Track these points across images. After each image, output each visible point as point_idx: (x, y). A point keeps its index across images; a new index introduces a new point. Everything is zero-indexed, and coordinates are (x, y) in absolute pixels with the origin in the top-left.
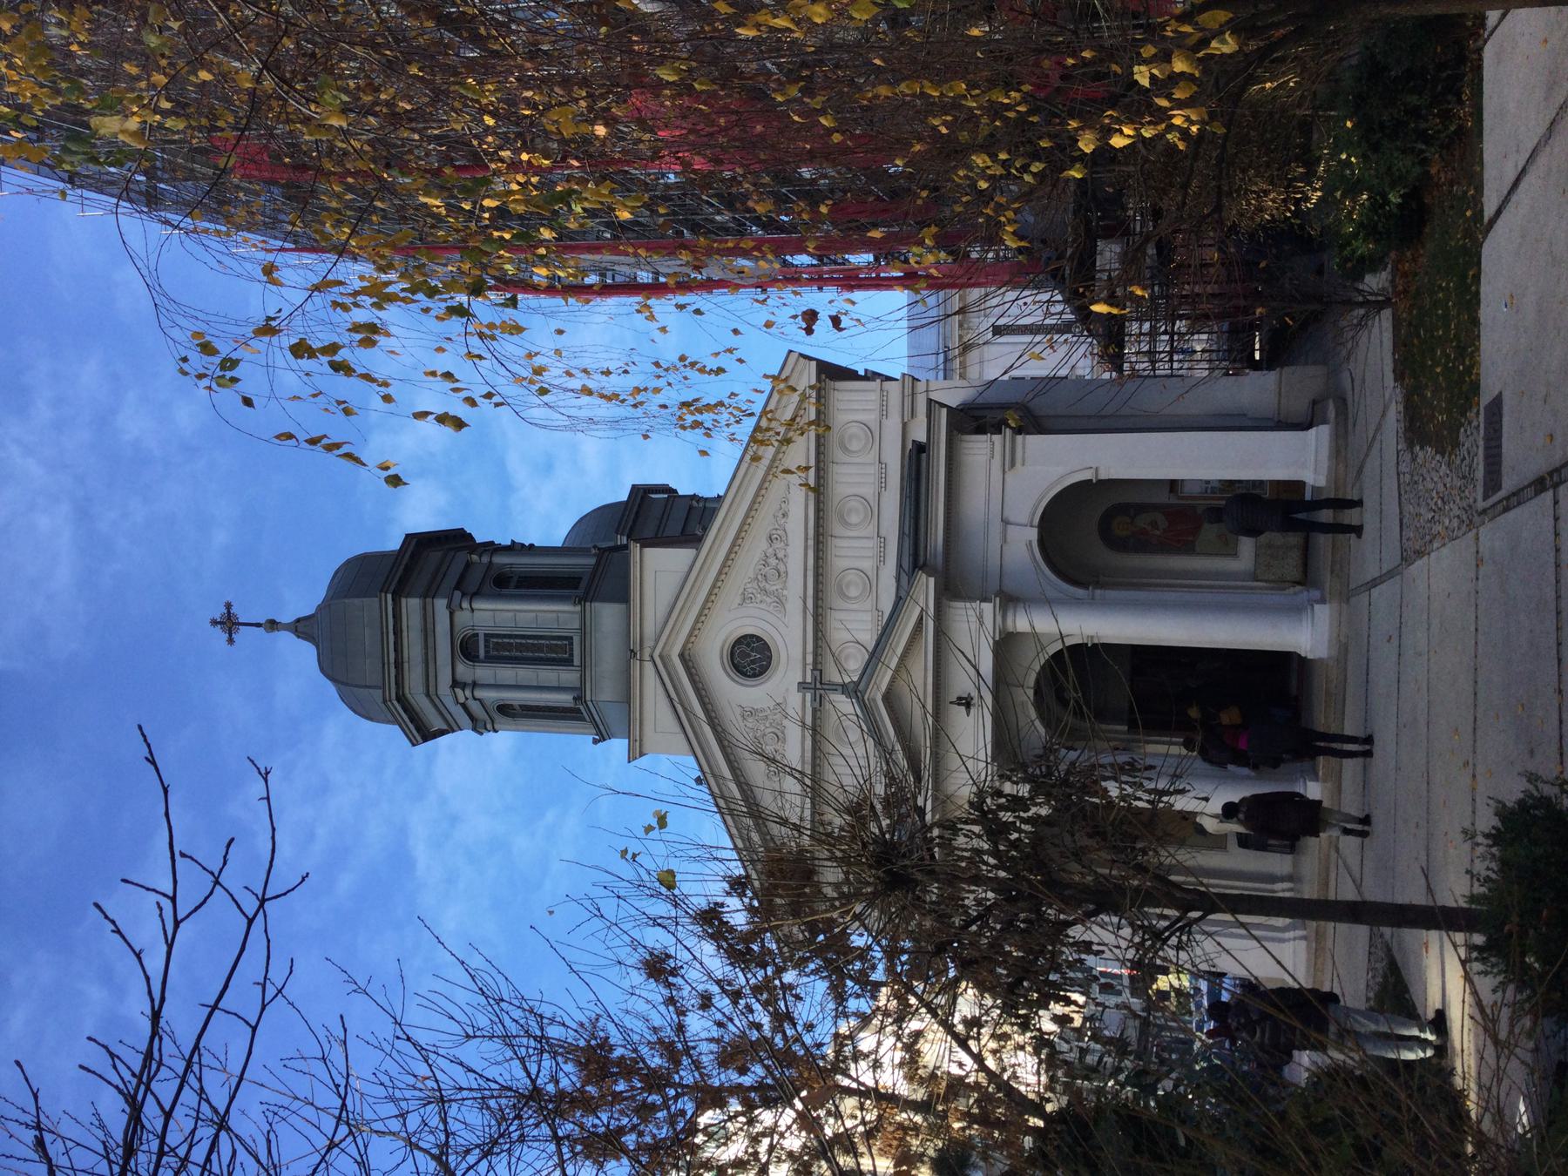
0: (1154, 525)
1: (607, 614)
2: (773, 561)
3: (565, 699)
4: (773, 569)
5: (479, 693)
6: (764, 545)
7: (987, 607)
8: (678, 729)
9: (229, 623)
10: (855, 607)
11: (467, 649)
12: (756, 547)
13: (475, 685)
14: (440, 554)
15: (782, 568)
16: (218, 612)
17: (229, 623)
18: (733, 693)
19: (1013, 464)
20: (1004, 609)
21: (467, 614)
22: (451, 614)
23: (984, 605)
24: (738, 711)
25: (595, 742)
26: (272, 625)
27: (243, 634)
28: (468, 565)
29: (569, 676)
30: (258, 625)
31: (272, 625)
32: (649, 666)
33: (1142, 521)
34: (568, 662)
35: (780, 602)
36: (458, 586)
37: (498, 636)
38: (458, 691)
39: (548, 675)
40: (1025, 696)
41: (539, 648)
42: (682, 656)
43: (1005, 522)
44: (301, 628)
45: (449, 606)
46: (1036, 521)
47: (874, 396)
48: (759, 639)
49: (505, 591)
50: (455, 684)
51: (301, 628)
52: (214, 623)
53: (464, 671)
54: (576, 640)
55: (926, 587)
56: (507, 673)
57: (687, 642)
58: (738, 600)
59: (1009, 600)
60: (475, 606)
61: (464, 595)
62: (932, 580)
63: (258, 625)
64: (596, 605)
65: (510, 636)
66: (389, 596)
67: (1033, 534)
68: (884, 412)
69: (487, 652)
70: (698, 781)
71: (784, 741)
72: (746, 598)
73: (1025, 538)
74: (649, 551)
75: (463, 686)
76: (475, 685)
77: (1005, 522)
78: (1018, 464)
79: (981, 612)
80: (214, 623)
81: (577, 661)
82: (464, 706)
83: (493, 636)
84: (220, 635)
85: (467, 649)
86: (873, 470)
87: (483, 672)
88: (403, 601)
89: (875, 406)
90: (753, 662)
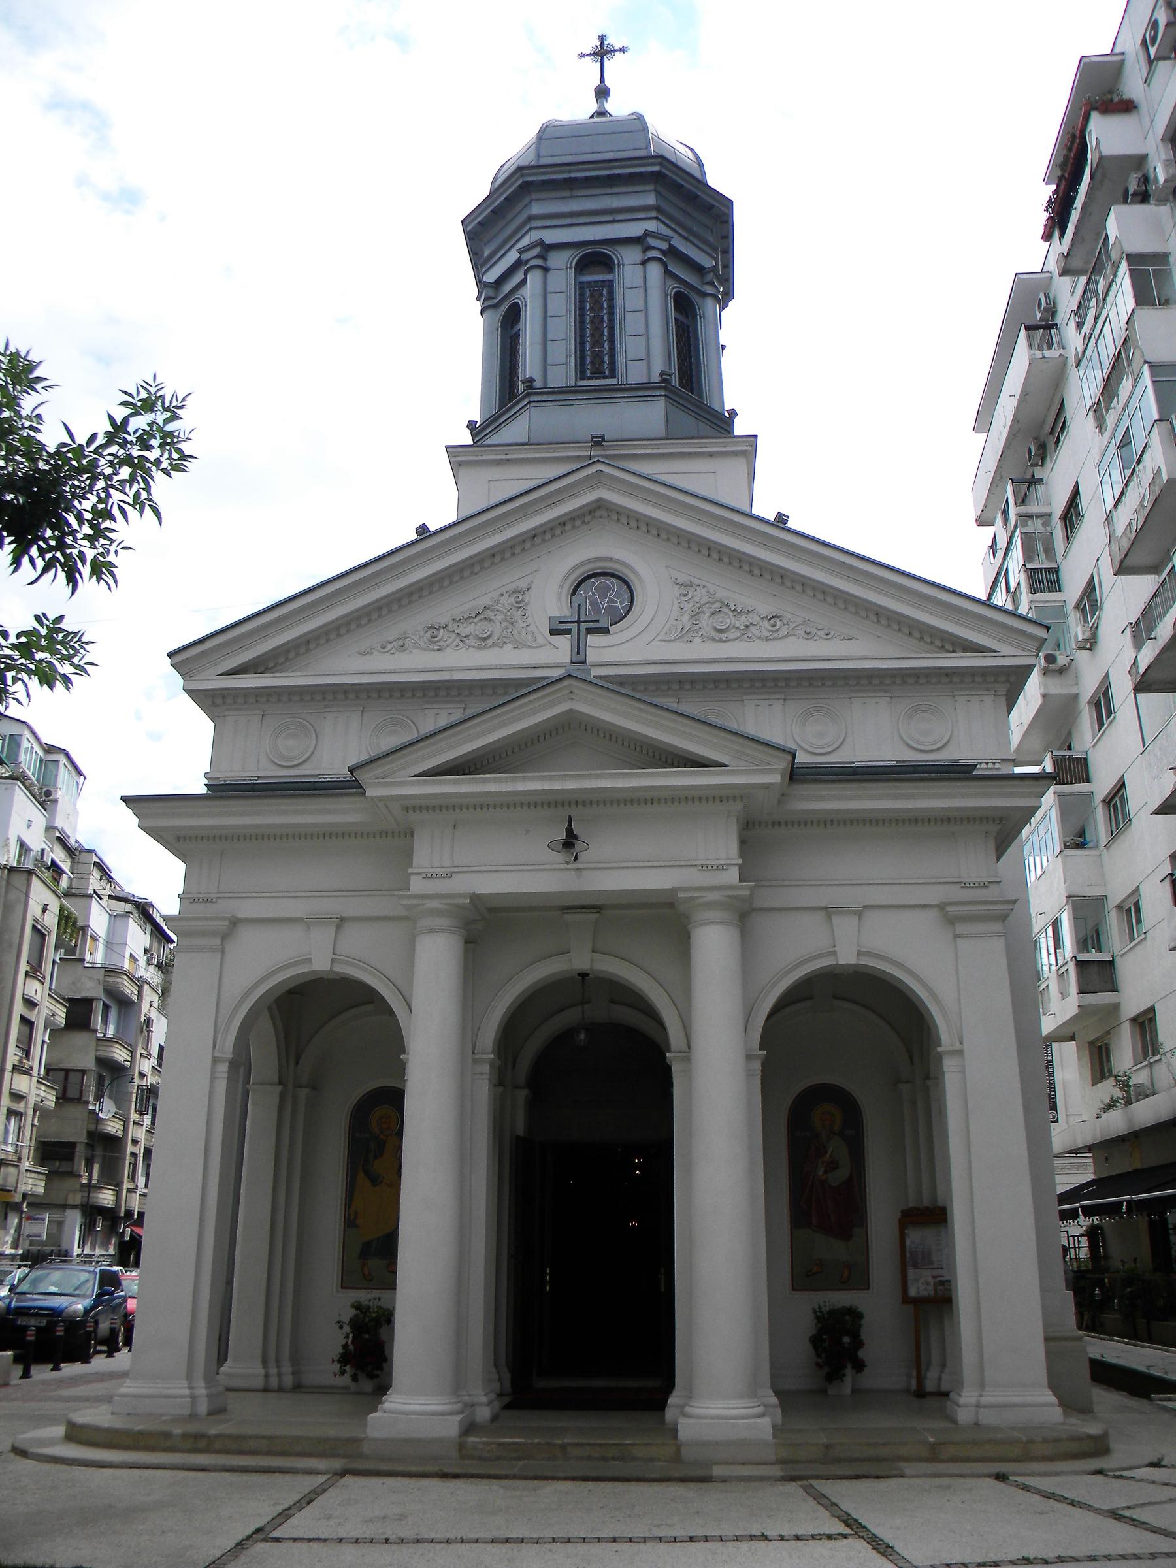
0: (833, 1166)
3: (529, 366)
7: (732, 876)
8: (493, 502)
9: (602, 52)
13: (546, 270)
15: (732, 634)
16: (614, 41)
17: (602, 52)
24: (522, 584)
25: (471, 425)
29: (561, 376)
30: (602, 80)
33: (837, 1149)
35: (685, 636)
41: (597, 342)
42: (600, 504)
45: (647, 234)
46: (865, 961)
50: (547, 248)
52: (602, 38)
54: (613, 381)
58: (683, 578)
61: (663, 252)
62: (776, 779)
63: (602, 80)
65: (611, 307)
66: (657, 168)
67: (847, 957)
71: (480, 648)
76: (546, 270)
79: (723, 867)
80: (602, 38)
88: (650, 187)
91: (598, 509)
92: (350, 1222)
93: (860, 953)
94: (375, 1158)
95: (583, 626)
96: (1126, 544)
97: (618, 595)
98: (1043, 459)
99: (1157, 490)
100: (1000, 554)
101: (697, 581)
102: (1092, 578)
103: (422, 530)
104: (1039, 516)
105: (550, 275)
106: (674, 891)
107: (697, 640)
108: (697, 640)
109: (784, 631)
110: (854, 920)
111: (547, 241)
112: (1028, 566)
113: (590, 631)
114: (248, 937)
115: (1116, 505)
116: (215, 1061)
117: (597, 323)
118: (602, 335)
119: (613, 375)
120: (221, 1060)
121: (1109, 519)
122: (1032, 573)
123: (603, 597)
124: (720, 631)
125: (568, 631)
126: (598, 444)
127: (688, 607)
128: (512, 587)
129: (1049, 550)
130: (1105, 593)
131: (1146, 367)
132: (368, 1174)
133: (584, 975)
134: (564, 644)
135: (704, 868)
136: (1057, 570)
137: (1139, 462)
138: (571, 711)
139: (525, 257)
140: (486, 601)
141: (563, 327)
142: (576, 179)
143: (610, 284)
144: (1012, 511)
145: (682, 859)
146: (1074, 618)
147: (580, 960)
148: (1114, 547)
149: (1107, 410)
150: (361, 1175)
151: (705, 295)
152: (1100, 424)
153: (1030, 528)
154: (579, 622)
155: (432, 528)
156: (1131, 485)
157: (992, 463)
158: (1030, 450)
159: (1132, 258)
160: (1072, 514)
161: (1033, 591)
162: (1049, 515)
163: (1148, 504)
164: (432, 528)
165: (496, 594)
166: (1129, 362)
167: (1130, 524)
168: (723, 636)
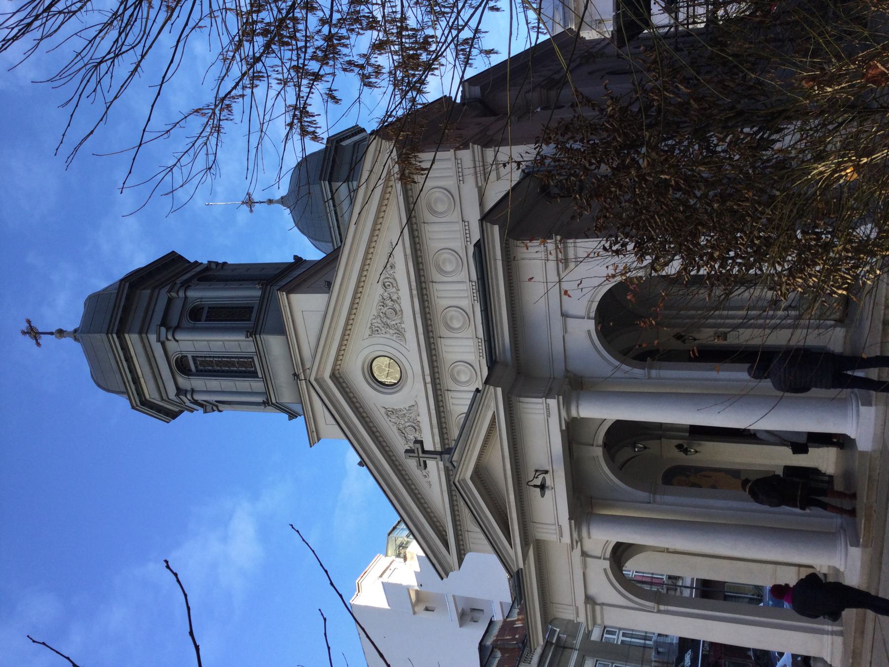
1: (274, 344)
4: (389, 306)
6: (380, 290)
7: (553, 403)
10: (459, 335)
12: (374, 293)
13: (193, 391)
14: (148, 292)
15: (398, 308)
20: (567, 404)
21: (174, 342)
22: (163, 344)
24: (383, 411)
27: (44, 339)
28: (170, 300)
29: (257, 385)
34: (253, 374)
35: (400, 333)
36: (164, 323)
43: (565, 315)
45: (158, 340)
46: (593, 315)
47: (451, 164)
49: (199, 324)
51: (76, 334)
57: (335, 365)
58: (368, 332)
60: (177, 338)
61: (168, 330)
62: (499, 390)
64: (264, 336)
66: (115, 336)
67: (591, 325)
68: (461, 178)
69: (196, 367)
70: (360, 464)
72: (374, 331)
74: (294, 297)
75: (185, 392)
77: (565, 315)
81: (260, 376)
85: (181, 366)
86: (458, 227)
87: (198, 383)
88: (127, 336)
89: (452, 173)
91: (336, 377)
93: (589, 318)
101: (369, 325)
103: (360, 464)
106: (562, 431)
107: (403, 326)
108: (403, 326)
111: (175, 391)
114: (592, 591)
116: (659, 611)
127: (384, 330)
128: (386, 417)
134: (431, 464)
135: (548, 415)
138: (471, 478)
140: (395, 429)
142: (133, 379)
145: (544, 421)
151: (186, 297)
154: (419, 457)
155: (359, 460)
164: (359, 460)
165: (390, 424)
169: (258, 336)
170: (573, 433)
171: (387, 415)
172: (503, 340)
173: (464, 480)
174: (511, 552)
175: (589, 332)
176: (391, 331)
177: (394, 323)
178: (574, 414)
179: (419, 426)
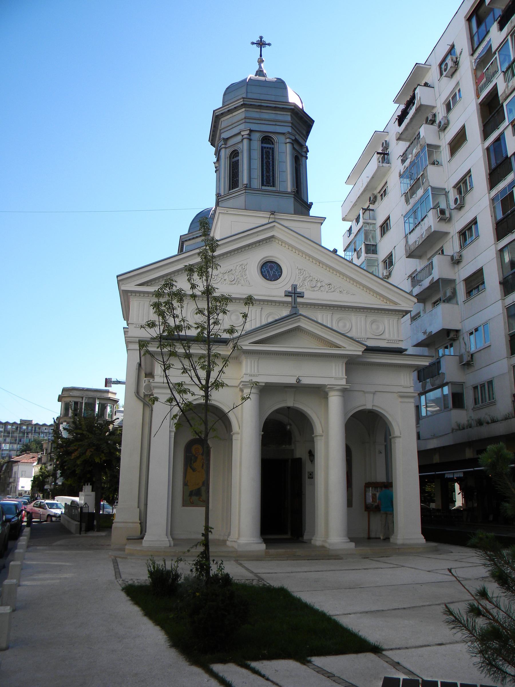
2: (319, 285)
5: (245, 142)
7: (343, 382)
11: (266, 139)
15: (316, 289)
16: (266, 40)
18: (254, 260)
19: (401, 397)
23: (345, 380)
26: (261, 61)
29: (256, 183)
30: (261, 56)
31: (261, 61)
32: (266, 221)
37: (273, 153)
38: (248, 132)
39: (257, 173)
40: (290, 401)
41: (268, 172)
42: (273, 237)
43: (374, 393)
44: (260, 72)
45: (289, 133)
46: (375, 408)
48: (280, 276)
52: (261, 38)
53: (257, 137)
55: (357, 350)
56: (257, 155)
59: (345, 392)
60: (288, 144)
61: (293, 140)
62: (361, 353)
63: (261, 56)
67: (369, 407)
69: (265, 147)
71: (230, 284)
73: (368, 403)
75: (249, 135)
76: (250, 140)
77: (374, 393)
78: (400, 400)
79: (341, 379)
80: (261, 38)
81: (264, 188)
82: (239, 133)
83: (273, 151)
84: (256, 39)
87: (257, 145)
88: (289, 113)
90: (268, 272)
92: (185, 484)
93: (373, 406)
94: (194, 462)
95: (296, 295)
96: (413, 248)
97: (276, 270)
98: (374, 202)
99: (429, 233)
100: (352, 236)
102: (392, 252)
104: (371, 224)
105: (252, 141)
109: (333, 290)
110: (372, 395)
112: (366, 243)
113: (298, 297)
115: (410, 233)
116: (170, 431)
117: (268, 163)
118: (270, 169)
119: (274, 186)
120: (172, 431)
121: (406, 236)
122: (367, 245)
123: (271, 270)
124: (312, 287)
125: (291, 296)
126: (273, 214)
129: (374, 238)
130: (397, 260)
131: (430, 188)
132: (191, 467)
133: (289, 408)
136: (376, 245)
137: (422, 220)
139: (243, 133)
141: (257, 164)
143: (273, 149)
144: (361, 220)
146: (381, 265)
147: (290, 403)
148: (408, 248)
149: (411, 197)
150: (189, 467)
152: (407, 201)
153: (367, 228)
154: (295, 293)
156: (418, 228)
157: (354, 198)
158: (370, 198)
159: (428, 145)
160: (385, 227)
161: (367, 253)
162: (375, 224)
163: (424, 237)
166: (423, 183)
167: (416, 242)
168: (313, 289)
169: (293, 196)
170: (320, 392)
171: (242, 265)
172: (373, 358)
173: (299, 321)
174: (247, 343)
175: (365, 405)
176: (300, 281)
177: (306, 284)
178: (331, 394)
179: (235, 284)
